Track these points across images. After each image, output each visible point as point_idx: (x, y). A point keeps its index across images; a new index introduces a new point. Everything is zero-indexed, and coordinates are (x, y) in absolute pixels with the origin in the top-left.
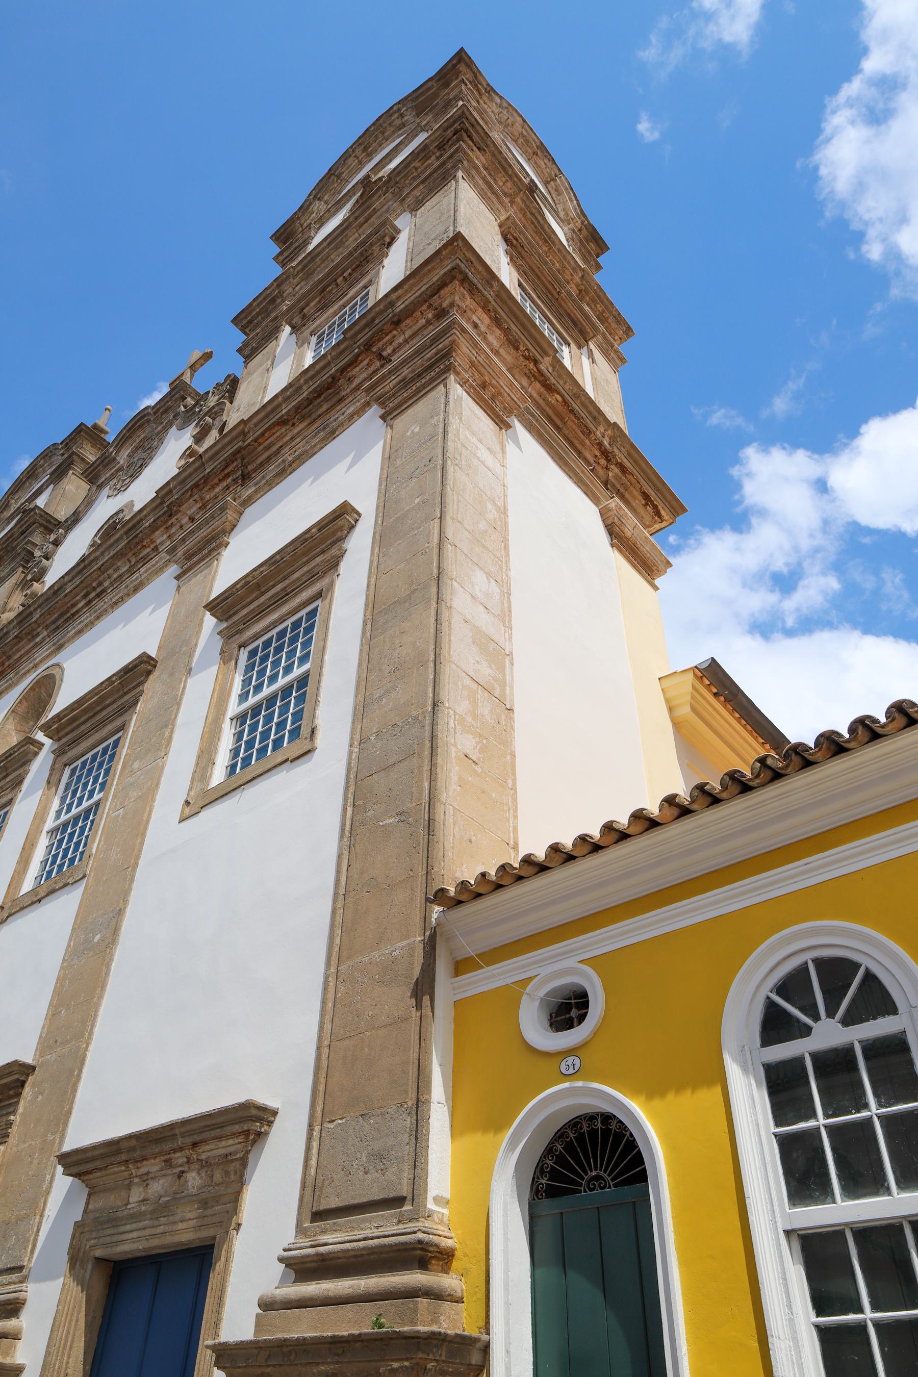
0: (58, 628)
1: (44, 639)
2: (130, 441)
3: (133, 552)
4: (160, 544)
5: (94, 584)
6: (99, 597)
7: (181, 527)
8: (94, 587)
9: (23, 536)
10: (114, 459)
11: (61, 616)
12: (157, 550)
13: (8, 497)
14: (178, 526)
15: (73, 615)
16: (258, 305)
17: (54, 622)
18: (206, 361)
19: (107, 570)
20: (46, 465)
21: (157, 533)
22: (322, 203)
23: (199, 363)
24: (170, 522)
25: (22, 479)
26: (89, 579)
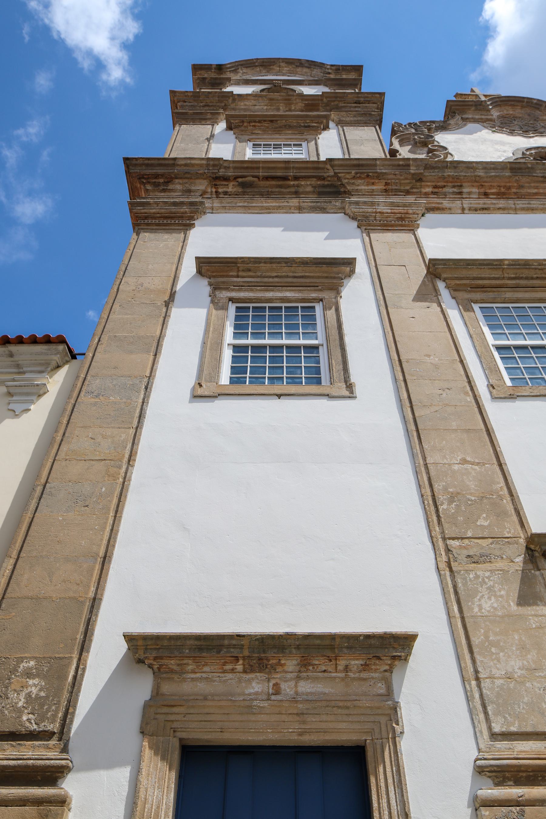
9: (355, 105)
10: (489, 110)
13: (238, 66)
20: (285, 69)
25: (255, 63)
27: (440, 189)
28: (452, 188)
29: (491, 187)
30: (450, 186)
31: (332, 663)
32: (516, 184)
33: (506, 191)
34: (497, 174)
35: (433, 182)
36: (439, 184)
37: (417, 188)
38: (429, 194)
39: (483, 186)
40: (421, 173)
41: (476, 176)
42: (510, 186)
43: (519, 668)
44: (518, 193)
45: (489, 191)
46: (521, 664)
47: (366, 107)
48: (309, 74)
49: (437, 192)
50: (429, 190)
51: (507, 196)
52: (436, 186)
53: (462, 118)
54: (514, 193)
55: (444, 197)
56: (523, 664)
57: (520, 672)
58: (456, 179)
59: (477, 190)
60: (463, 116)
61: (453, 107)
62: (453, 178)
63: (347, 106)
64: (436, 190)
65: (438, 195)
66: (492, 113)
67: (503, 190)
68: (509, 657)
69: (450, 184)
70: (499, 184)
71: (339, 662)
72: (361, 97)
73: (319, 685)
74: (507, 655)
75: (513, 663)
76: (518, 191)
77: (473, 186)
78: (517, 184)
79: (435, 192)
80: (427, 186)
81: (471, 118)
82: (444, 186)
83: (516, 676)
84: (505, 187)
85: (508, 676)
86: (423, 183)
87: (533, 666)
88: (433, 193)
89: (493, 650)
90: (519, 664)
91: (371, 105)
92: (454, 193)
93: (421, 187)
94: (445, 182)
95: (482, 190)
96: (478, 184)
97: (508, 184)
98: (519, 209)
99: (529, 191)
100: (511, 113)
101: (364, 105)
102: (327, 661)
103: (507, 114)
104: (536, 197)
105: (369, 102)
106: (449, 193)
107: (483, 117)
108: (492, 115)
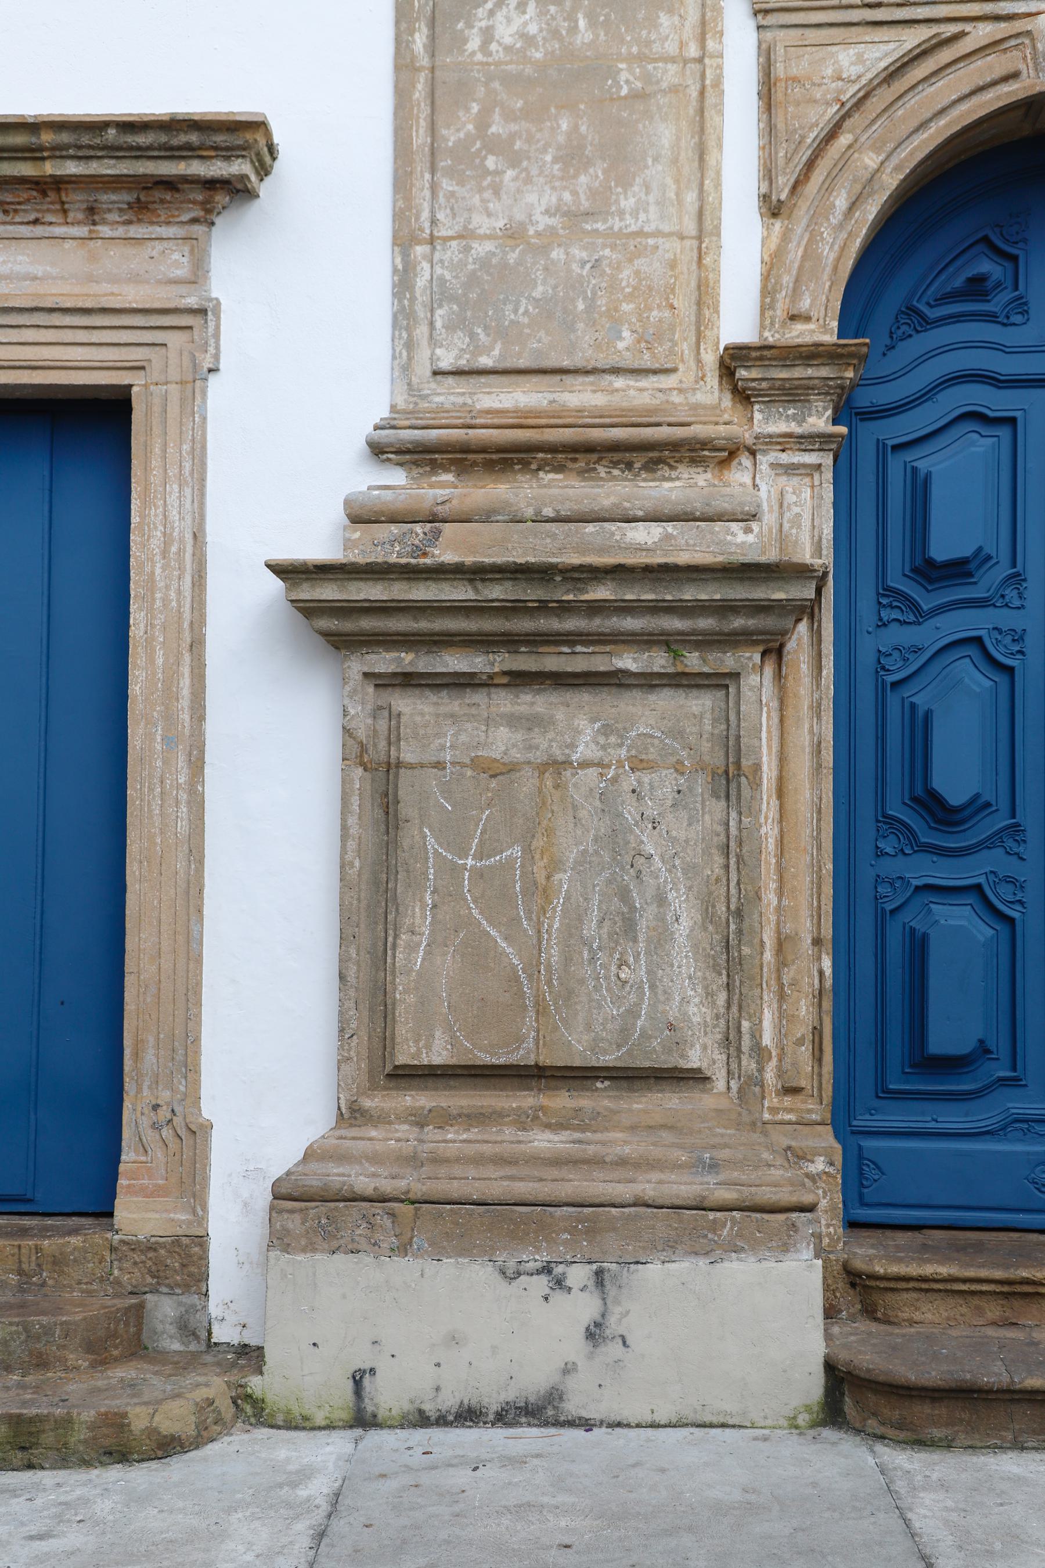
31: (48, 199)
43: (547, 212)
46: (554, 199)
56: (560, 199)
57: (543, 222)
68: (528, 180)
71: (67, 195)
73: (20, 258)
74: (524, 175)
75: (531, 198)
83: (531, 232)
85: (510, 232)
87: (585, 204)
89: (491, 162)
90: (550, 198)
102: (35, 193)
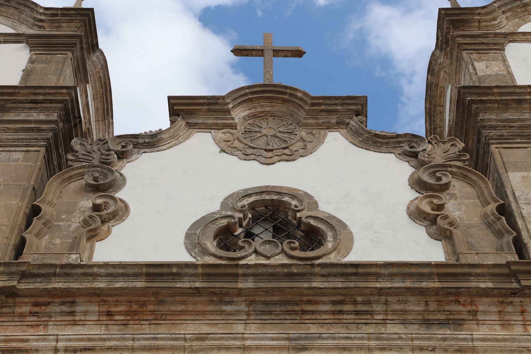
0: (270, 313)
1: (237, 313)
2: (250, 105)
3: (439, 298)
4: (483, 311)
5: (359, 299)
6: (356, 314)
7: (523, 312)
8: (356, 301)
10: (228, 112)
11: (282, 303)
12: (475, 315)
14: (519, 309)
15: (304, 312)
16: (500, 94)
17: (266, 303)
18: (293, 56)
19: (387, 295)
21: (485, 299)
22: (504, 16)
23: (285, 54)
24: (510, 299)
26: (357, 290)
27: (43, 308)
28: (60, 305)
29: (117, 303)
30: (58, 303)
32: (153, 299)
33: (139, 309)
34: (125, 286)
35: (33, 296)
36: (41, 300)
37: (10, 307)
38: (26, 316)
39: (105, 301)
40: (14, 287)
41: (94, 289)
42: (145, 301)
44: (156, 311)
45: (114, 309)
47: (47, 108)
48: (16, 17)
49: (38, 313)
50: (26, 309)
51: (141, 317)
52: (37, 302)
53: (187, 123)
54: (150, 311)
55: (48, 319)
58: (66, 292)
59: (96, 309)
60: (190, 121)
61: (175, 108)
62: (62, 291)
63: (18, 108)
64: (36, 309)
65: (38, 317)
66: (233, 116)
67: (135, 307)
69: (57, 300)
70: (128, 299)
72: (40, 94)
76: (156, 308)
77: (91, 302)
78: (156, 298)
79: (35, 313)
80: (25, 303)
81: (201, 124)
82: (49, 303)
84: (137, 302)
86: (18, 300)
88: (32, 314)
91: (54, 105)
92: (62, 313)
93: (15, 305)
94: (50, 297)
95: (104, 309)
96: (98, 299)
97: (142, 299)
98: (138, 349)
99: (172, 308)
100: (268, 109)
101: (43, 105)
103: (262, 112)
104: (183, 317)
105: (51, 101)
106: (55, 313)
107: (219, 121)
108: (233, 119)
